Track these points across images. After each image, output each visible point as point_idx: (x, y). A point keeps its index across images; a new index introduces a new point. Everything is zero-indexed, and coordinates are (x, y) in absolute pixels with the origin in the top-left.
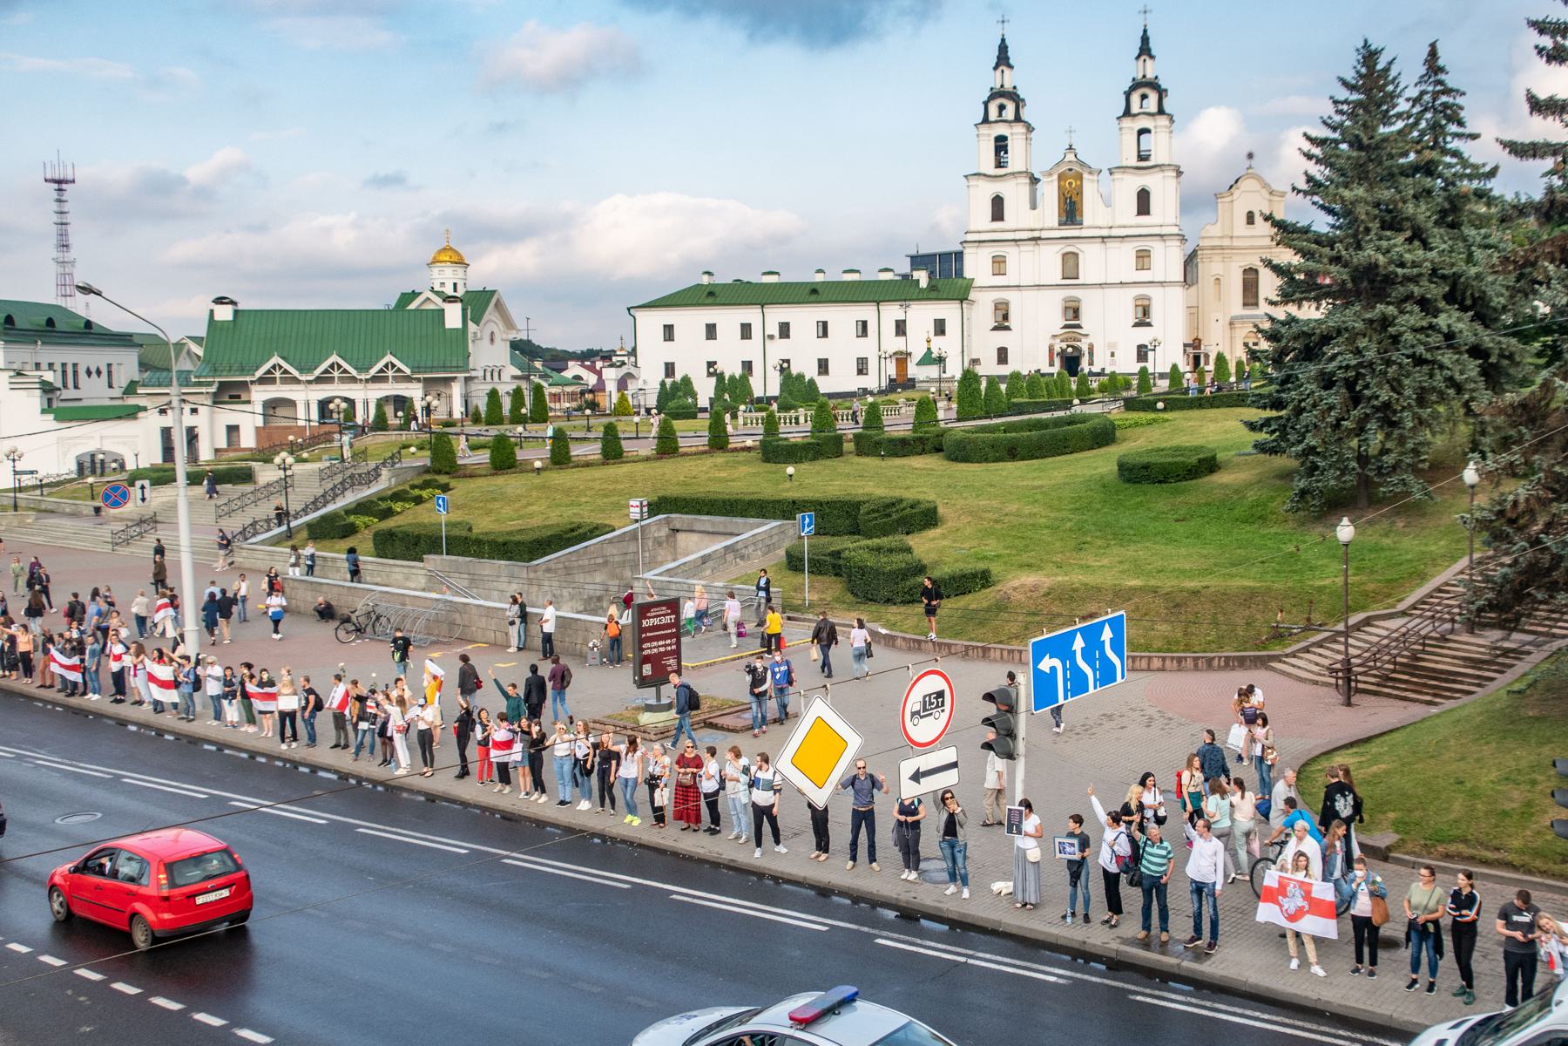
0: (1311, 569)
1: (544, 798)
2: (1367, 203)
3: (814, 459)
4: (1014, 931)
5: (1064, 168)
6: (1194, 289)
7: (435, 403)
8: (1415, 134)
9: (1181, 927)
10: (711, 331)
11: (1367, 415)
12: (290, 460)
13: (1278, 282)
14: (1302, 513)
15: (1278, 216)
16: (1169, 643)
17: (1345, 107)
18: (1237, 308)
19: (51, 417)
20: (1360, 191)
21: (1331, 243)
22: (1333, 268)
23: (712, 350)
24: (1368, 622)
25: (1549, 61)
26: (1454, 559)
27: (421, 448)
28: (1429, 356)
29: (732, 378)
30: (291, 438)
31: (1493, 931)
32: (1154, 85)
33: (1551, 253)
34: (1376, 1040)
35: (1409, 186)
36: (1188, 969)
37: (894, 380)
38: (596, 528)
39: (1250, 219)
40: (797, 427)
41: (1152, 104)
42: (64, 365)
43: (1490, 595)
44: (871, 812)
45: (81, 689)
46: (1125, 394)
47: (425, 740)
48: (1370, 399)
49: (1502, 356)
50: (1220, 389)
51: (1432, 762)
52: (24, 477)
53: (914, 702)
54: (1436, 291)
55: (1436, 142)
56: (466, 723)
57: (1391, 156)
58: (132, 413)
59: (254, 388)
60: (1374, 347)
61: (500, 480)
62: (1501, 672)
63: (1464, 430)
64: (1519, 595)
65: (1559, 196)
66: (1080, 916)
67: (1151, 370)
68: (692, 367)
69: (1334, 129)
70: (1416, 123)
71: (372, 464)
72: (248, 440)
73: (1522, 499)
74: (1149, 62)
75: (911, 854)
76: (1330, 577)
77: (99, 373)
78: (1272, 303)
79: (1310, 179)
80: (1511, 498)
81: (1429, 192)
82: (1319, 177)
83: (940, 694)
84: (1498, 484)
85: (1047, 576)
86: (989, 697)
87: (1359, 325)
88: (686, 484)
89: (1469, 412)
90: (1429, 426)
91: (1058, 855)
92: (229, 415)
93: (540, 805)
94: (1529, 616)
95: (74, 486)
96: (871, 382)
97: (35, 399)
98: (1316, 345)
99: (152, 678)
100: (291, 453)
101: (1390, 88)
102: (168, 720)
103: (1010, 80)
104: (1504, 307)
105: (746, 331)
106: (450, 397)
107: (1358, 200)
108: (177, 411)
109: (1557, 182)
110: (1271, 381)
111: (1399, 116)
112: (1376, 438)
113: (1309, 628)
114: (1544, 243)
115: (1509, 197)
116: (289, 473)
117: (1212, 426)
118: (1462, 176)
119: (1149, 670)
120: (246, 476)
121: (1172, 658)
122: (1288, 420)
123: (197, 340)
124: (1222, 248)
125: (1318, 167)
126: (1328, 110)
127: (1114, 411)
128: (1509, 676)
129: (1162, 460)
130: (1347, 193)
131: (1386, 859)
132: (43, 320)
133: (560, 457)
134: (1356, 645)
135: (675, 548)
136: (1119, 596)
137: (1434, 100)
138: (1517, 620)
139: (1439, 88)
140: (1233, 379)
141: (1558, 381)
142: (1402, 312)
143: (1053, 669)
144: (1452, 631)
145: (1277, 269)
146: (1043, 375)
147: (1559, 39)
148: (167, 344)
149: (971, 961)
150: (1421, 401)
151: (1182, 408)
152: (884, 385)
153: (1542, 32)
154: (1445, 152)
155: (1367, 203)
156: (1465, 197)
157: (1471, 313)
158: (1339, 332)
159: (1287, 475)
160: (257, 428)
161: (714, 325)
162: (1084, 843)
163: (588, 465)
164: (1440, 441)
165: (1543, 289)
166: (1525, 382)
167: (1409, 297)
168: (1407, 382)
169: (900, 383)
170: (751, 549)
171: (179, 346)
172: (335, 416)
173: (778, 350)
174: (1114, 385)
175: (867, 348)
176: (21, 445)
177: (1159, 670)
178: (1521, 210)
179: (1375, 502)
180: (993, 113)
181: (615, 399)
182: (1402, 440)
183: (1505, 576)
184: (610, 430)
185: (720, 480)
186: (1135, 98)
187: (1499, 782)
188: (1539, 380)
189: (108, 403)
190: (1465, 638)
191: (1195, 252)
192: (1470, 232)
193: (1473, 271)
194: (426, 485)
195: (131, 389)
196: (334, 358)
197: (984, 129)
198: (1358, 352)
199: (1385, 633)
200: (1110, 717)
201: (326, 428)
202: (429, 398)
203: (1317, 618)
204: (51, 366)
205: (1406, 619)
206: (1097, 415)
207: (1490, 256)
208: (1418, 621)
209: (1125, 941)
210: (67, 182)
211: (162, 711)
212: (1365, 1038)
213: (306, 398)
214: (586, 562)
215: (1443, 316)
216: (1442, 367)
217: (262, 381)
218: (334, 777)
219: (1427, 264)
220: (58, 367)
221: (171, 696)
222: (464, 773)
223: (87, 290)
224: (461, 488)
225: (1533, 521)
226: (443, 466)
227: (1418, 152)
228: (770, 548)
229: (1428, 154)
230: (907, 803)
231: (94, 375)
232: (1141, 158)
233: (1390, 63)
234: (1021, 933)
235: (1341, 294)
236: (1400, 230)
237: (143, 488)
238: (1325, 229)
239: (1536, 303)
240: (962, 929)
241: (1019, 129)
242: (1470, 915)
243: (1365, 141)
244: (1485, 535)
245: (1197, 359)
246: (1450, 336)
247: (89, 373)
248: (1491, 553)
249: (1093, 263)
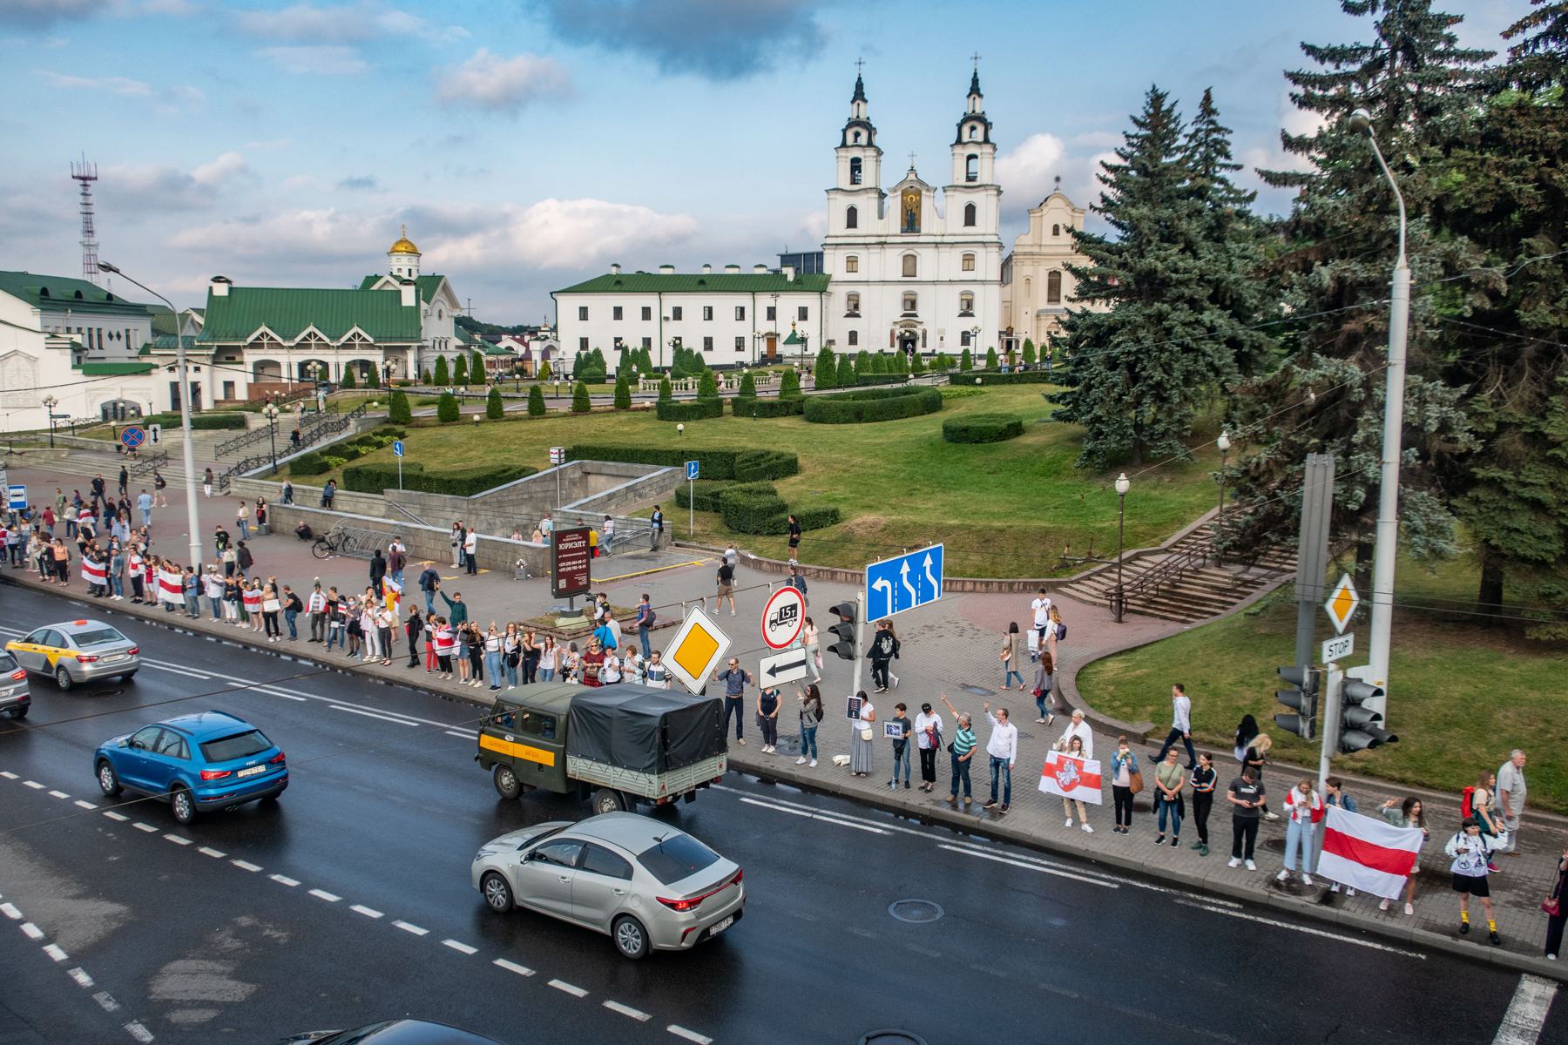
0: (1094, 514)
1: (479, 684)
2: (1150, 220)
3: (700, 418)
4: (850, 794)
5: (906, 186)
6: (1008, 287)
7: (393, 366)
8: (1191, 164)
9: (981, 792)
10: (618, 313)
11: (1143, 392)
12: (275, 410)
13: (1076, 283)
14: (1089, 469)
15: (1078, 229)
16: (979, 570)
17: (1135, 141)
18: (1042, 301)
19: (81, 371)
20: (1145, 210)
21: (1120, 252)
22: (1121, 272)
23: (618, 329)
24: (1137, 557)
25: (1300, 107)
26: (1208, 509)
27: (382, 403)
28: (1195, 346)
29: (635, 351)
30: (276, 392)
31: (1225, 799)
32: (981, 119)
33: (1295, 264)
34: (1130, 882)
35: (1184, 206)
36: (987, 826)
38: (523, 470)
39: (1056, 230)
40: (686, 392)
41: (979, 134)
42: (90, 329)
43: (1235, 537)
44: (741, 699)
45: (107, 590)
46: (950, 371)
47: (385, 635)
48: (1146, 379)
49: (1253, 346)
50: (1026, 368)
51: (1184, 667)
52: (59, 420)
53: (773, 612)
54: (1202, 293)
55: (1207, 171)
56: (415, 625)
57: (1170, 182)
58: (146, 370)
59: (246, 352)
60: (1151, 337)
61: (446, 430)
62: (1241, 598)
63: (1220, 405)
64: (1258, 538)
65: (1303, 218)
66: (902, 783)
67: (972, 352)
68: (602, 341)
69: (1126, 158)
70: (1192, 156)
71: (342, 415)
72: (241, 394)
73: (1263, 461)
74: (978, 99)
75: (770, 733)
76: (1108, 521)
78: (1071, 300)
79: (1105, 199)
80: (1255, 460)
81: (1199, 212)
82: (1112, 198)
83: (794, 607)
84: (1244, 449)
85: (884, 515)
86: (834, 610)
87: (1140, 319)
88: (596, 436)
89: (1225, 391)
90: (1193, 401)
91: (886, 735)
92: (224, 373)
93: (476, 688)
94: (1265, 554)
95: (99, 428)
96: (747, 356)
97: (66, 358)
98: (1105, 334)
99: (163, 584)
100: (277, 405)
101: (1172, 126)
102: (177, 617)
103: (865, 111)
104: (1256, 307)
105: (646, 314)
106: (406, 362)
107: (1143, 217)
108: (183, 369)
109: (1303, 206)
110: (1068, 362)
111: (1178, 149)
112: (1150, 411)
113: (1090, 560)
114: (1290, 256)
115: (1265, 218)
116: (274, 421)
117: (1020, 398)
118: (1227, 200)
119: (963, 591)
120: (240, 423)
121: (982, 583)
122: (1080, 394)
123: (199, 311)
124: (1032, 254)
125: (1112, 190)
126: (1122, 143)
127: (942, 384)
128: (1247, 601)
129: (979, 425)
130: (1133, 212)
131: (1144, 743)
132: (72, 292)
133: (495, 412)
134: (1128, 575)
135: (586, 487)
136: (941, 532)
137: (1207, 136)
138: (1255, 558)
139: (1211, 127)
140: (1037, 361)
141: (1296, 368)
142: (1174, 309)
143: (884, 588)
144: (1204, 565)
145: (1076, 273)
146: (885, 354)
147: (1309, 88)
148: (173, 313)
149: (815, 816)
150: (1187, 381)
151: (996, 383)
153: (1296, 82)
154: (1214, 179)
155: (1150, 220)
156: (1228, 217)
157: (1229, 312)
158: (1123, 324)
159: (1077, 439)
161: (620, 308)
162: (907, 726)
163: (517, 419)
164: (1200, 414)
165: (1286, 293)
166: (1270, 368)
167: (1180, 297)
168: (1176, 366)
169: (771, 358)
170: (647, 489)
171: (185, 316)
172: (312, 375)
173: (673, 329)
174: (942, 363)
175: (744, 329)
176: (56, 394)
177: (971, 591)
178: (1273, 228)
179: (1146, 461)
180: (850, 140)
181: (539, 367)
182: (1170, 413)
183: (1247, 523)
184: (535, 391)
185: (623, 433)
186: (966, 129)
187: (1235, 684)
188: (1281, 367)
189: (127, 361)
190: (1214, 571)
191: (1010, 256)
192: (1232, 245)
193: (1233, 277)
194: (385, 433)
195: (145, 350)
196: (311, 329)
197: (842, 152)
198: (1138, 341)
199: (1151, 565)
200: (931, 628)
201: (305, 385)
202: (388, 363)
203: (1096, 552)
204: (79, 330)
205: (1168, 555)
206: (927, 387)
207: (1246, 265)
208: (1177, 556)
209: (937, 803)
210: (90, 179)
211: (173, 610)
212: (1121, 880)
213: (288, 361)
214: (515, 497)
215: (1207, 313)
216: (1204, 354)
217: (253, 346)
218: (311, 664)
219: (1196, 271)
220: (85, 331)
221: (178, 599)
222: (415, 662)
223: (107, 268)
224: (414, 435)
225: (1271, 480)
226: (399, 418)
227: (1192, 179)
228: (662, 489)
229: (1200, 181)
230: (768, 692)
231: (115, 338)
232: (969, 179)
233: (1173, 105)
234: (855, 795)
235: (1126, 293)
236: (1176, 242)
237: (155, 430)
238: (1115, 241)
239: (1282, 304)
240: (811, 791)
241: (871, 152)
242: (1208, 787)
243: (1150, 169)
244: (1233, 489)
245: (1009, 344)
246: (1211, 329)
247: (111, 336)
248: (1237, 504)
249: (930, 264)
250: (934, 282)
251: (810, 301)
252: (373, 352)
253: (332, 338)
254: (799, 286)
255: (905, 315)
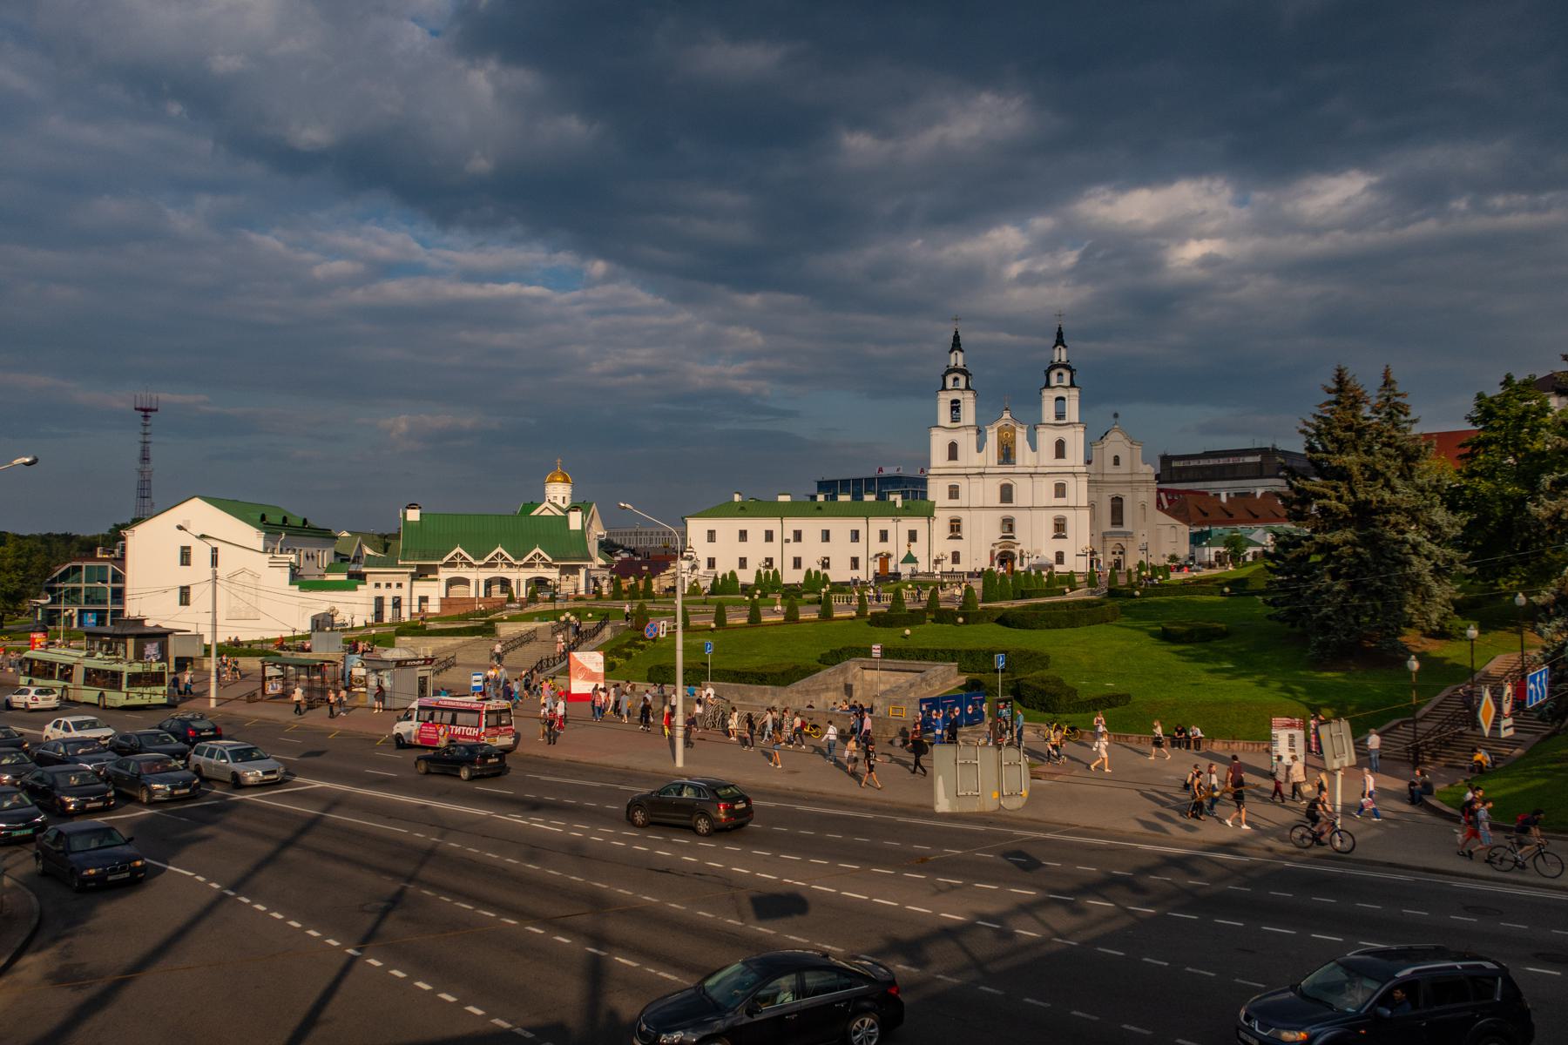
10: (743, 535)
19: (297, 587)
23: (743, 549)
37: (878, 574)
59: (441, 570)
72: (434, 608)
77: (313, 557)
92: (421, 588)
96: (861, 574)
105: (769, 536)
152: (871, 577)
160: (441, 598)
161: (745, 532)
169: (884, 577)
173: (793, 550)
175: (858, 550)
189: (316, 578)
213: (478, 576)
214: (816, 688)
217: (447, 565)
247: (308, 557)
250: (1029, 508)
251: (918, 524)
252: (550, 570)
253: (517, 559)
254: (907, 512)
255: (1003, 537)
